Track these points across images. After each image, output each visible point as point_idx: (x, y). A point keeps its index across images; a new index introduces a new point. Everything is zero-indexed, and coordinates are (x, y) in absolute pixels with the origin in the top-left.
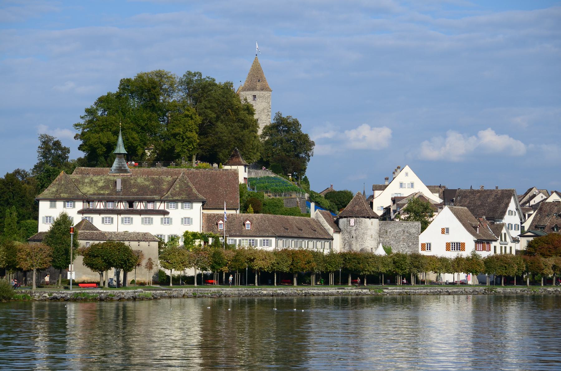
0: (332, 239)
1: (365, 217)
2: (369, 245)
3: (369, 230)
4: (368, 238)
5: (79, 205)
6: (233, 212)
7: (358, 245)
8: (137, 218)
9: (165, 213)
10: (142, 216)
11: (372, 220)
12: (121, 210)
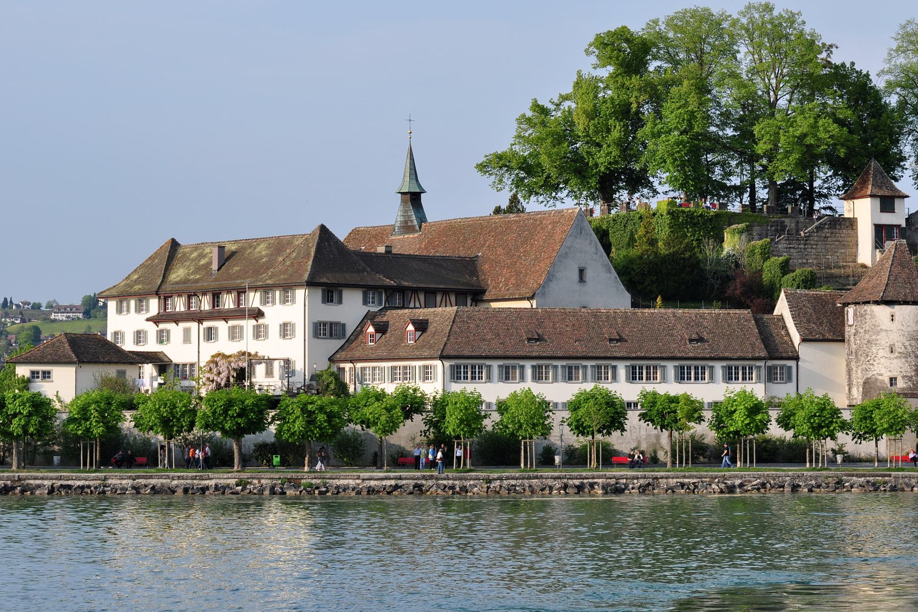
0: (797, 358)
1: (868, 302)
2: (883, 371)
3: (883, 334)
4: (881, 353)
5: (154, 306)
6: (525, 304)
7: (859, 372)
8: (222, 327)
9: (258, 314)
10: (232, 323)
11: (898, 309)
12: (180, 314)
